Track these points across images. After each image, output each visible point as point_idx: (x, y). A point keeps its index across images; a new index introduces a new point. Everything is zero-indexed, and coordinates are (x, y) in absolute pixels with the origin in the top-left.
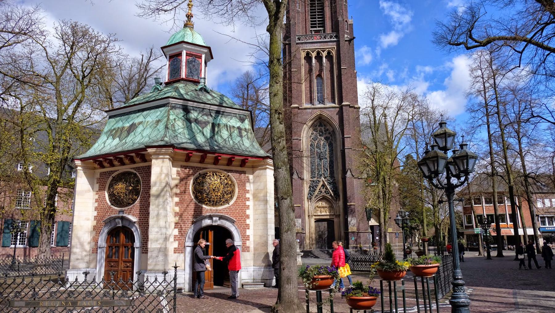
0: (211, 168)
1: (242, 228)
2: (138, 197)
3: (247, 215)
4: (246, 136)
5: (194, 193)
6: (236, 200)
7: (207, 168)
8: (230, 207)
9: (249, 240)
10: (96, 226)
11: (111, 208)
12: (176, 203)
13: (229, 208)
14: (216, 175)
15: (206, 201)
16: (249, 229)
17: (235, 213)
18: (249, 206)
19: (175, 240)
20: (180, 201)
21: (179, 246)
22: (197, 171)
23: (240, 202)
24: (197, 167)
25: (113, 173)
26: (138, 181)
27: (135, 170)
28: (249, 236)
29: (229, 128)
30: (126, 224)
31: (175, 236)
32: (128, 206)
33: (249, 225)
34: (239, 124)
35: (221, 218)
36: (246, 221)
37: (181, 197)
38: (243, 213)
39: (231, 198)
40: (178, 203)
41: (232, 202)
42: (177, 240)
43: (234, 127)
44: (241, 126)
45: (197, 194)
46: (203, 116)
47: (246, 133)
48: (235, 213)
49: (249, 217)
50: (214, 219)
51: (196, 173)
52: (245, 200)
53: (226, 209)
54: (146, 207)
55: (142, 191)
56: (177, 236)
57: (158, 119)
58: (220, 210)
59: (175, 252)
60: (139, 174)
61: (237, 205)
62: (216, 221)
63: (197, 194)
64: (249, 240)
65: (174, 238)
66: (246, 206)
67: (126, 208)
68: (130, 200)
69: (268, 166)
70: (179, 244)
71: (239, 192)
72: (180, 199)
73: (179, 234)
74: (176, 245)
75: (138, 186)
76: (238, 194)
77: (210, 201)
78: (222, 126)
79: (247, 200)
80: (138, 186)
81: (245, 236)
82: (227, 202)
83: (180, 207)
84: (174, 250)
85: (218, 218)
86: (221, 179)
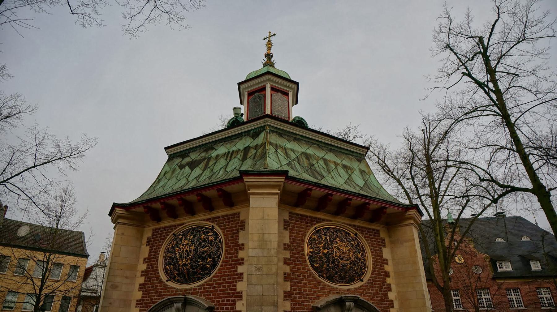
0: (189, 222)
3: (238, 293)
7: (183, 224)
8: (210, 281)
13: (209, 283)
17: (217, 291)
18: (242, 274)
22: (171, 232)
23: (227, 268)
24: (170, 226)
36: (235, 304)
38: (231, 290)
40: (143, 284)
43: (239, 150)
44: (251, 145)
47: (255, 151)
48: (217, 291)
50: (176, 305)
51: (168, 235)
53: (203, 285)
58: (195, 289)
61: (221, 276)
66: (237, 274)
69: (252, 191)
71: (226, 250)
72: (145, 278)
76: (225, 254)
79: (240, 264)
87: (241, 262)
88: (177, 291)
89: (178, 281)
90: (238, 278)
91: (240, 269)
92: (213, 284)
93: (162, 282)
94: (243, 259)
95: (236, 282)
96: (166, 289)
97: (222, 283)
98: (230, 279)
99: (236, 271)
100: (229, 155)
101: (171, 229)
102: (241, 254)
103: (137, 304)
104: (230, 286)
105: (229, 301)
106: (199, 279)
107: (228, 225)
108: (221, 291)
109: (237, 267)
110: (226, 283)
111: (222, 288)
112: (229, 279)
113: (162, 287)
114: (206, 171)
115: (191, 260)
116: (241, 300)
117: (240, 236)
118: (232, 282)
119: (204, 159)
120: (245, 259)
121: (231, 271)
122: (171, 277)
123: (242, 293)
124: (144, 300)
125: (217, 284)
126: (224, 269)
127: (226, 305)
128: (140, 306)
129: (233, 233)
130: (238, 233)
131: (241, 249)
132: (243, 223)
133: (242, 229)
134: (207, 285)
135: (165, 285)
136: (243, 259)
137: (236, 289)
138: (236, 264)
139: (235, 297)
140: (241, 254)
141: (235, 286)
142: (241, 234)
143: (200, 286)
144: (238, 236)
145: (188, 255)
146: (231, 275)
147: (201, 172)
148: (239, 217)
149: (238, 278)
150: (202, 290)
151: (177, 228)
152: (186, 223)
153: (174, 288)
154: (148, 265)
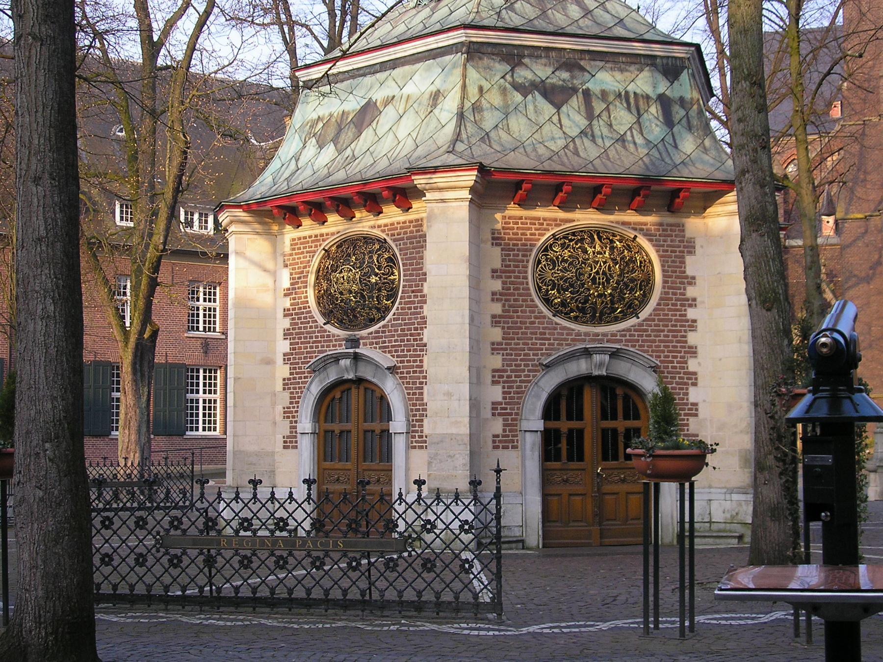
1: (677, 383)
2: (393, 303)
3: (690, 347)
4: (684, 121)
5: (540, 288)
6: (659, 304)
8: (640, 325)
9: (696, 415)
10: (289, 379)
11: (325, 331)
12: (494, 316)
13: (639, 328)
14: (600, 238)
15: (572, 311)
16: (695, 384)
17: (654, 341)
18: (695, 321)
19: (493, 415)
20: (503, 311)
21: (504, 431)
23: (670, 310)
24: (545, 219)
25: (324, 240)
26: (392, 260)
27: (383, 231)
28: (696, 404)
29: (632, 100)
30: (366, 373)
31: (493, 403)
32: (371, 326)
33: (695, 373)
34: (663, 87)
35: (615, 354)
36: (686, 363)
37: (506, 300)
38: (678, 342)
39: (644, 300)
41: (644, 314)
42: (499, 415)
45: (547, 291)
46: (557, 73)
47: (682, 113)
49: (695, 353)
50: (597, 358)
51: (543, 235)
52: (682, 305)
53: (629, 330)
54: (416, 329)
55: (404, 286)
56: (501, 403)
57: (435, 90)
58: (613, 335)
59: (496, 447)
60: (394, 240)
61: (659, 320)
62: (601, 365)
63: (547, 291)
64: (696, 415)
65: (493, 409)
66: (687, 321)
67: (364, 333)
68: (374, 311)
70: (504, 425)
72: (504, 306)
73: (504, 398)
74: (497, 426)
75: (393, 274)
76: (664, 287)
77: (582, 310)
78: (611, 98)
79: (690, 306)
80: (393, 274)
81: (687, 404)
82: (632, 310)
83: (503, 328)
84: (494, 442)
85: (607, 357)
86: (612, 249)
87: (693, 303)
88: (579, 334)
89: (576, 318)
90: (689, 326)
91: (691, 313)
92: (646, 331)
93: (544, 317)
94: (694, 300)
95: (685, 331)
96: (555, 329)
97: (663, 331)
98: (676, 326)
99: (685, 315)
100: (632, 100)
101: (548, 225)
102: (690, 292)
103: (493, 349)
104: (676, 337)
105: (676, 357)
106: (616, 320)
107: (665, 241)
108: (661, 341)
109: (685, 310)
110: (669, 331)
111: (662, 338)
112: (672, 326)
113: (546, 325)
114: (595, 122)
115: (613, 290)
116: (696, 357)
117: (687, 263)
118: (680, 331)
119: (575, 90)
120: (698, 300)
121: (676, 315)
122: (562, 310)
123: (696, 347)
124: (506, 344)
125: (652, 331)
126: (663, 310)
127: (672, 362)
128: (501, 352)
129: (676, 256)
130: (683, 257)
131: (690, 284)
132: (691, 242)
133: (690, 253)
134: (635, 331)
135: (551, 322)
136: (694, 300)
137: (686, 342)
138: (684, 305)
139: (685, 352)
140: (690, 292)
141: (685, 337)
142: (689, 259)
143: (623, 330)
144: (684, 263)
145: (608, 281)
146: (676, 320)
147: (587, 123)
148: (683, 231)
149: (689, 326)
150: (628, 337)
151: (560, 225)
152: (578, 220)
153: (573, 330)
154: (504, 283)
